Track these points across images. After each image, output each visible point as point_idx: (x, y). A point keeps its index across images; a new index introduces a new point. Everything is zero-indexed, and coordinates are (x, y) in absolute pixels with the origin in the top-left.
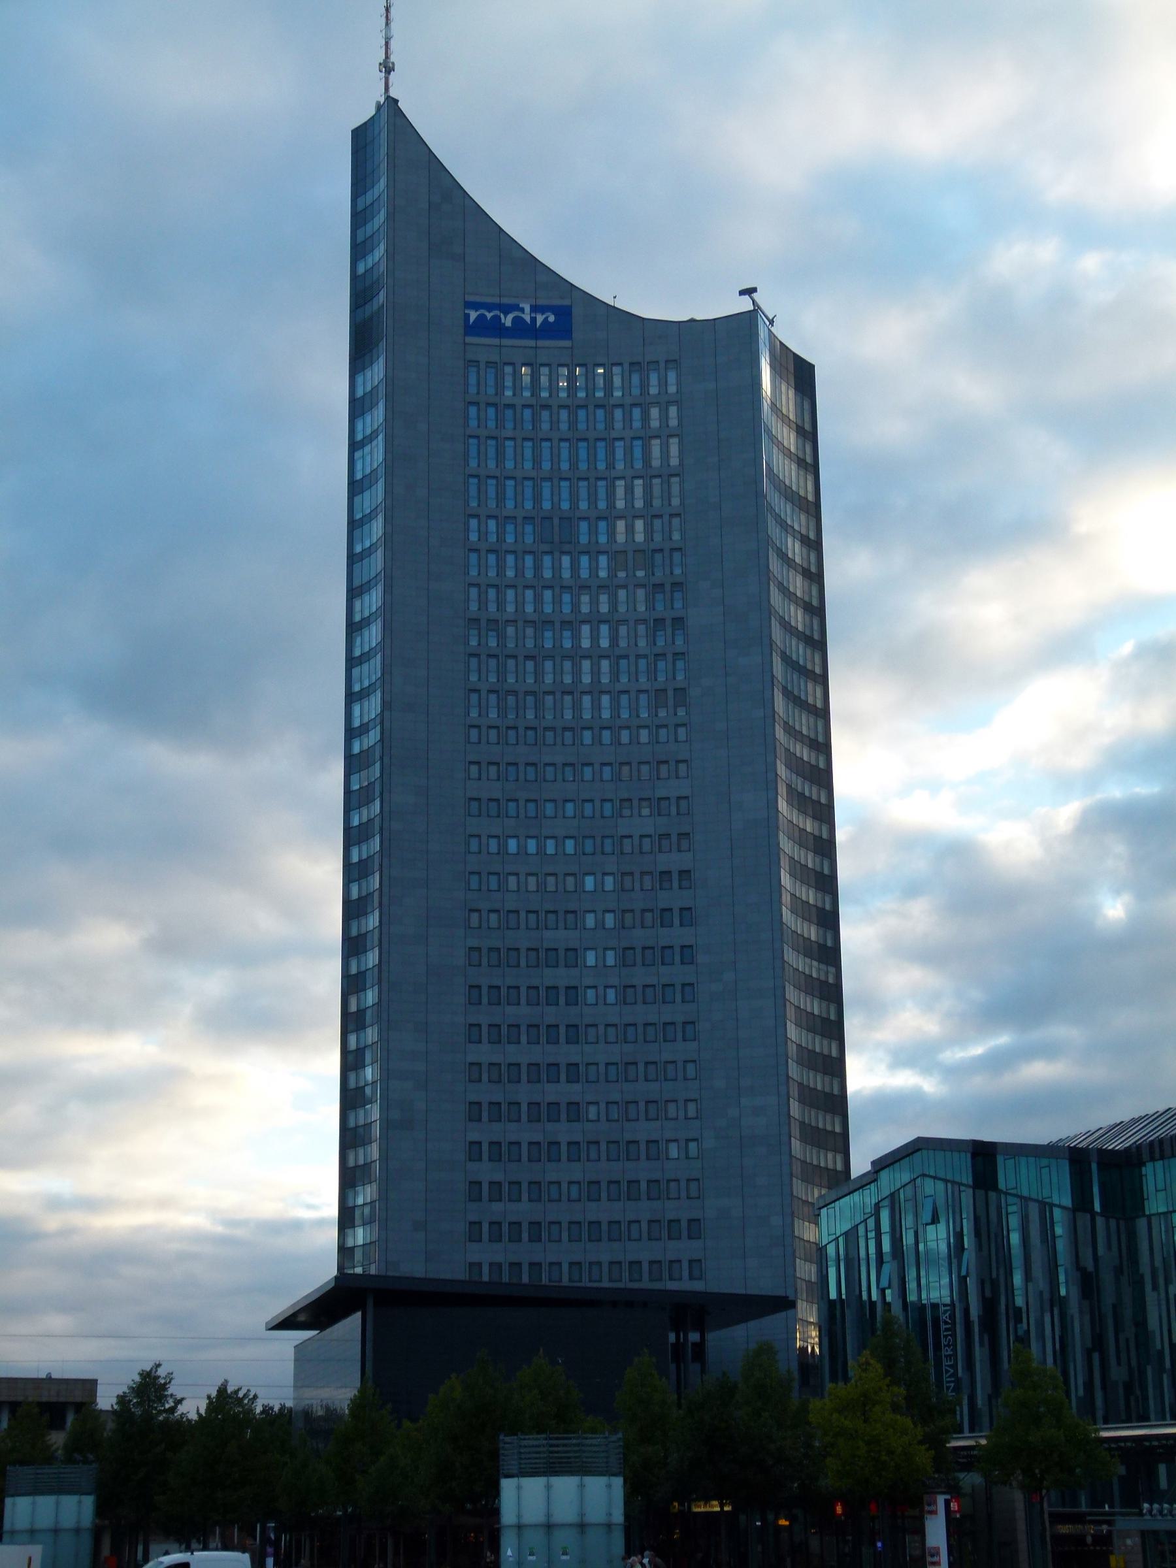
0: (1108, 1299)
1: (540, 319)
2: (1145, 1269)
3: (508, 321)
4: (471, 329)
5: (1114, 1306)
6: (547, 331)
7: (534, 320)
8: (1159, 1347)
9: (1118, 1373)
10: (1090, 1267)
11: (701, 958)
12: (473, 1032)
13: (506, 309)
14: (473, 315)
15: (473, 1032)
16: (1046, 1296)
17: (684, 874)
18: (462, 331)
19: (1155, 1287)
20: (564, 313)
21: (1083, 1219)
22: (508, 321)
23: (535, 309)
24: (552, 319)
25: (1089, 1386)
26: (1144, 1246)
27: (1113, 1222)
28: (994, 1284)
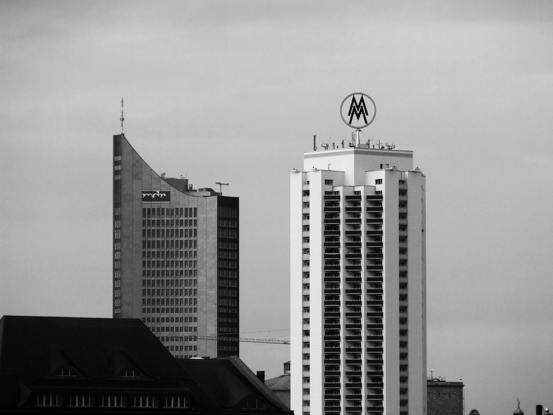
1: (162, 195)
3: (153, 196)
4: (144, 199)
6: (164, 199)
13: (153, 193)
14: (144, 195)
20: (168, 193)
22: (153, 196)
23: (160, 192)
24: (165, 195)
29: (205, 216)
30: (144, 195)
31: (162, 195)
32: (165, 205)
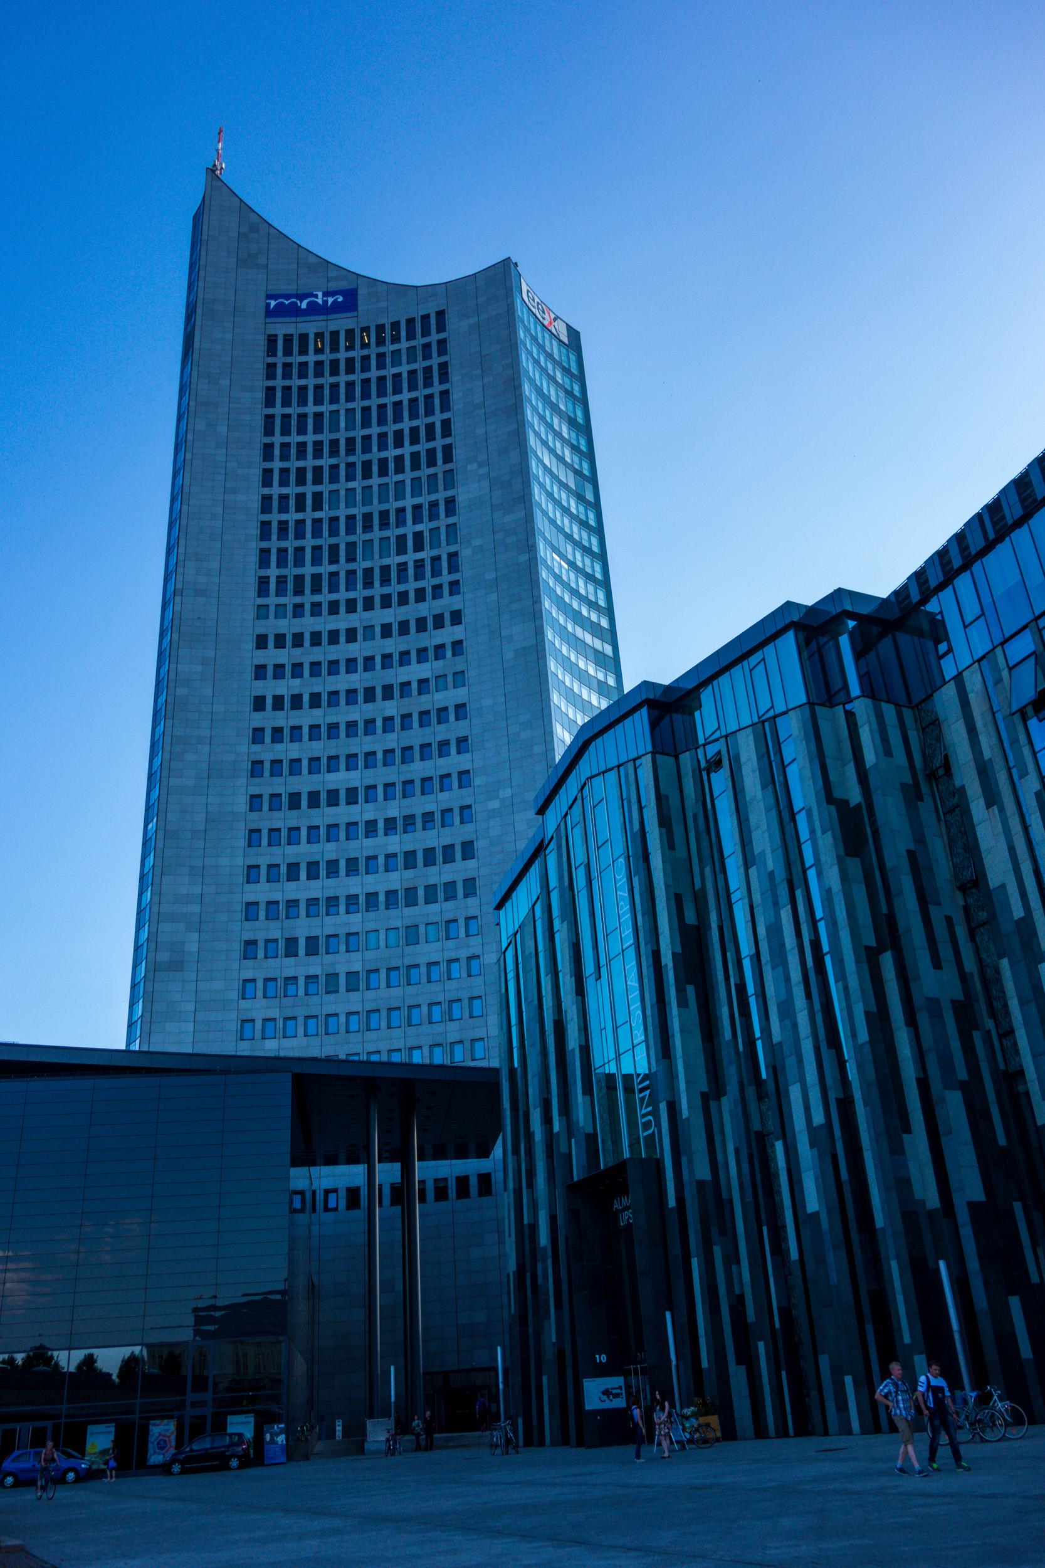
0: (896, 844)
1: (330, 300)
2: (966, 776)
5: (911, 854)
6: (337, 308)
7: (325, 302)
8: (1018, 912)
9: (936, 984)
10: (855, 796)
11: (477, 781)
12: (251, 873)
13: (302, 297)
14: (273, 303)
15: (251, 873)
16: (781, 875)
17: (460, 708)
18: (263, 315)
19: (992, 799)
21: (833, 720)
22: (304, 305)
23: (326, 294)
25: (879, 1019)
26: (956, 733)
27: (889, 710)
28: (699, 899)
29: (473, 320)
30: (273, 303)
31: (330, 300)
32: (341, 323)
